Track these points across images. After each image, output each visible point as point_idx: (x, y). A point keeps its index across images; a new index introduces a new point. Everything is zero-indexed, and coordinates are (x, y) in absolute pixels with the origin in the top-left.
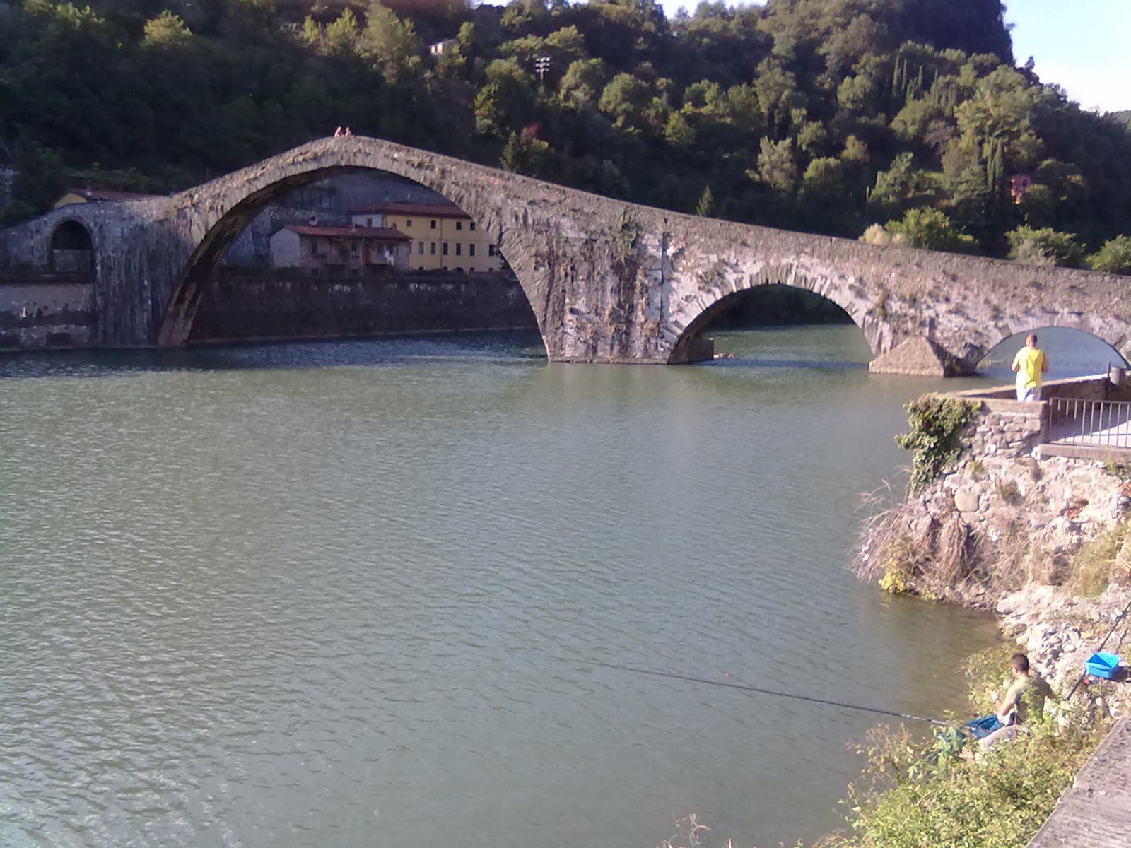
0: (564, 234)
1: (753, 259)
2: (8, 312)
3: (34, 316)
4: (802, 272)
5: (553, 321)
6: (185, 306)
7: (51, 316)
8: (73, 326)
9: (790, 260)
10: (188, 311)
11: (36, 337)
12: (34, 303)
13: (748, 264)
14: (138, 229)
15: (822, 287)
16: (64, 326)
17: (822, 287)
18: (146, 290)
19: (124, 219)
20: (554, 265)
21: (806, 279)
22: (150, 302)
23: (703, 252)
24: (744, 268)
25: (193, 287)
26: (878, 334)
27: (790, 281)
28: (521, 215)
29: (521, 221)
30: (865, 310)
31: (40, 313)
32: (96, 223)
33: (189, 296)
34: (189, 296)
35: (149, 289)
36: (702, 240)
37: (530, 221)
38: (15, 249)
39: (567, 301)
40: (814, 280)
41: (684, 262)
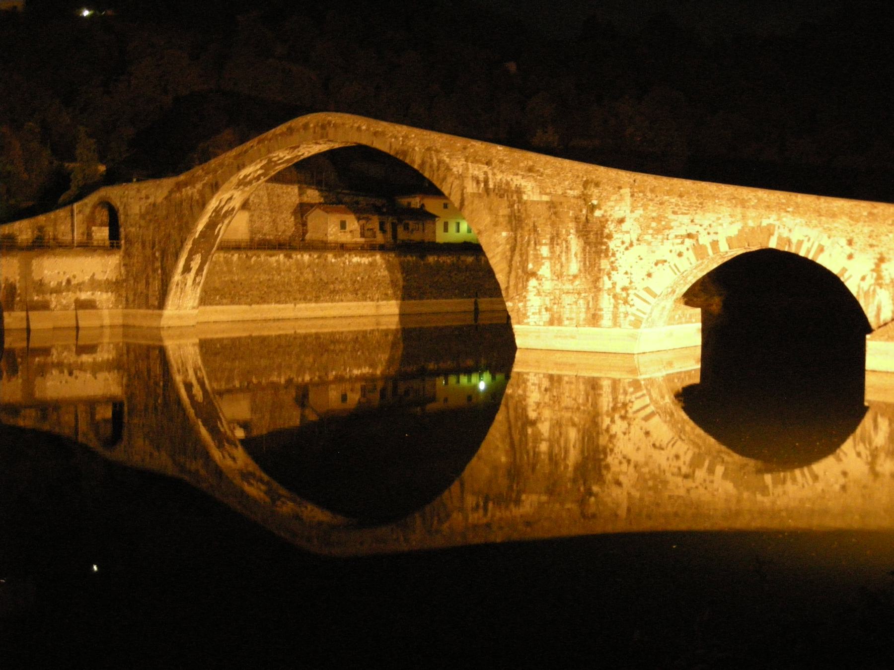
0: (525, 197)
1: (730, 220)
3: (64, 284)
4: (785, 234)
5: (516, 285)
8: (99, 293)
9: (771, 221)
10: (195, 280)
12: (64, 273)
13: (725, 225)
14: (152, 206)
15: (808, 251)
17: (808, 251)
18: (157, 260)
19: (142, 198)
20: (516, 230)
21: (789, 242)
22: (160, 271)
23: (674, 213)
24: (719, 229)
25: (198, 259)
26: (876, 303)
27: (773, 244)
28: (482, 177)
29: (482, 185)
30: (860, 277)
32: (121, 203)
33: (195, 265)
34: (195, 265)
35: (159, 259)
36: (673, 200)
37: (491, 186)
39: (530, 266)
40: (800, 243)
41: (654, 224)
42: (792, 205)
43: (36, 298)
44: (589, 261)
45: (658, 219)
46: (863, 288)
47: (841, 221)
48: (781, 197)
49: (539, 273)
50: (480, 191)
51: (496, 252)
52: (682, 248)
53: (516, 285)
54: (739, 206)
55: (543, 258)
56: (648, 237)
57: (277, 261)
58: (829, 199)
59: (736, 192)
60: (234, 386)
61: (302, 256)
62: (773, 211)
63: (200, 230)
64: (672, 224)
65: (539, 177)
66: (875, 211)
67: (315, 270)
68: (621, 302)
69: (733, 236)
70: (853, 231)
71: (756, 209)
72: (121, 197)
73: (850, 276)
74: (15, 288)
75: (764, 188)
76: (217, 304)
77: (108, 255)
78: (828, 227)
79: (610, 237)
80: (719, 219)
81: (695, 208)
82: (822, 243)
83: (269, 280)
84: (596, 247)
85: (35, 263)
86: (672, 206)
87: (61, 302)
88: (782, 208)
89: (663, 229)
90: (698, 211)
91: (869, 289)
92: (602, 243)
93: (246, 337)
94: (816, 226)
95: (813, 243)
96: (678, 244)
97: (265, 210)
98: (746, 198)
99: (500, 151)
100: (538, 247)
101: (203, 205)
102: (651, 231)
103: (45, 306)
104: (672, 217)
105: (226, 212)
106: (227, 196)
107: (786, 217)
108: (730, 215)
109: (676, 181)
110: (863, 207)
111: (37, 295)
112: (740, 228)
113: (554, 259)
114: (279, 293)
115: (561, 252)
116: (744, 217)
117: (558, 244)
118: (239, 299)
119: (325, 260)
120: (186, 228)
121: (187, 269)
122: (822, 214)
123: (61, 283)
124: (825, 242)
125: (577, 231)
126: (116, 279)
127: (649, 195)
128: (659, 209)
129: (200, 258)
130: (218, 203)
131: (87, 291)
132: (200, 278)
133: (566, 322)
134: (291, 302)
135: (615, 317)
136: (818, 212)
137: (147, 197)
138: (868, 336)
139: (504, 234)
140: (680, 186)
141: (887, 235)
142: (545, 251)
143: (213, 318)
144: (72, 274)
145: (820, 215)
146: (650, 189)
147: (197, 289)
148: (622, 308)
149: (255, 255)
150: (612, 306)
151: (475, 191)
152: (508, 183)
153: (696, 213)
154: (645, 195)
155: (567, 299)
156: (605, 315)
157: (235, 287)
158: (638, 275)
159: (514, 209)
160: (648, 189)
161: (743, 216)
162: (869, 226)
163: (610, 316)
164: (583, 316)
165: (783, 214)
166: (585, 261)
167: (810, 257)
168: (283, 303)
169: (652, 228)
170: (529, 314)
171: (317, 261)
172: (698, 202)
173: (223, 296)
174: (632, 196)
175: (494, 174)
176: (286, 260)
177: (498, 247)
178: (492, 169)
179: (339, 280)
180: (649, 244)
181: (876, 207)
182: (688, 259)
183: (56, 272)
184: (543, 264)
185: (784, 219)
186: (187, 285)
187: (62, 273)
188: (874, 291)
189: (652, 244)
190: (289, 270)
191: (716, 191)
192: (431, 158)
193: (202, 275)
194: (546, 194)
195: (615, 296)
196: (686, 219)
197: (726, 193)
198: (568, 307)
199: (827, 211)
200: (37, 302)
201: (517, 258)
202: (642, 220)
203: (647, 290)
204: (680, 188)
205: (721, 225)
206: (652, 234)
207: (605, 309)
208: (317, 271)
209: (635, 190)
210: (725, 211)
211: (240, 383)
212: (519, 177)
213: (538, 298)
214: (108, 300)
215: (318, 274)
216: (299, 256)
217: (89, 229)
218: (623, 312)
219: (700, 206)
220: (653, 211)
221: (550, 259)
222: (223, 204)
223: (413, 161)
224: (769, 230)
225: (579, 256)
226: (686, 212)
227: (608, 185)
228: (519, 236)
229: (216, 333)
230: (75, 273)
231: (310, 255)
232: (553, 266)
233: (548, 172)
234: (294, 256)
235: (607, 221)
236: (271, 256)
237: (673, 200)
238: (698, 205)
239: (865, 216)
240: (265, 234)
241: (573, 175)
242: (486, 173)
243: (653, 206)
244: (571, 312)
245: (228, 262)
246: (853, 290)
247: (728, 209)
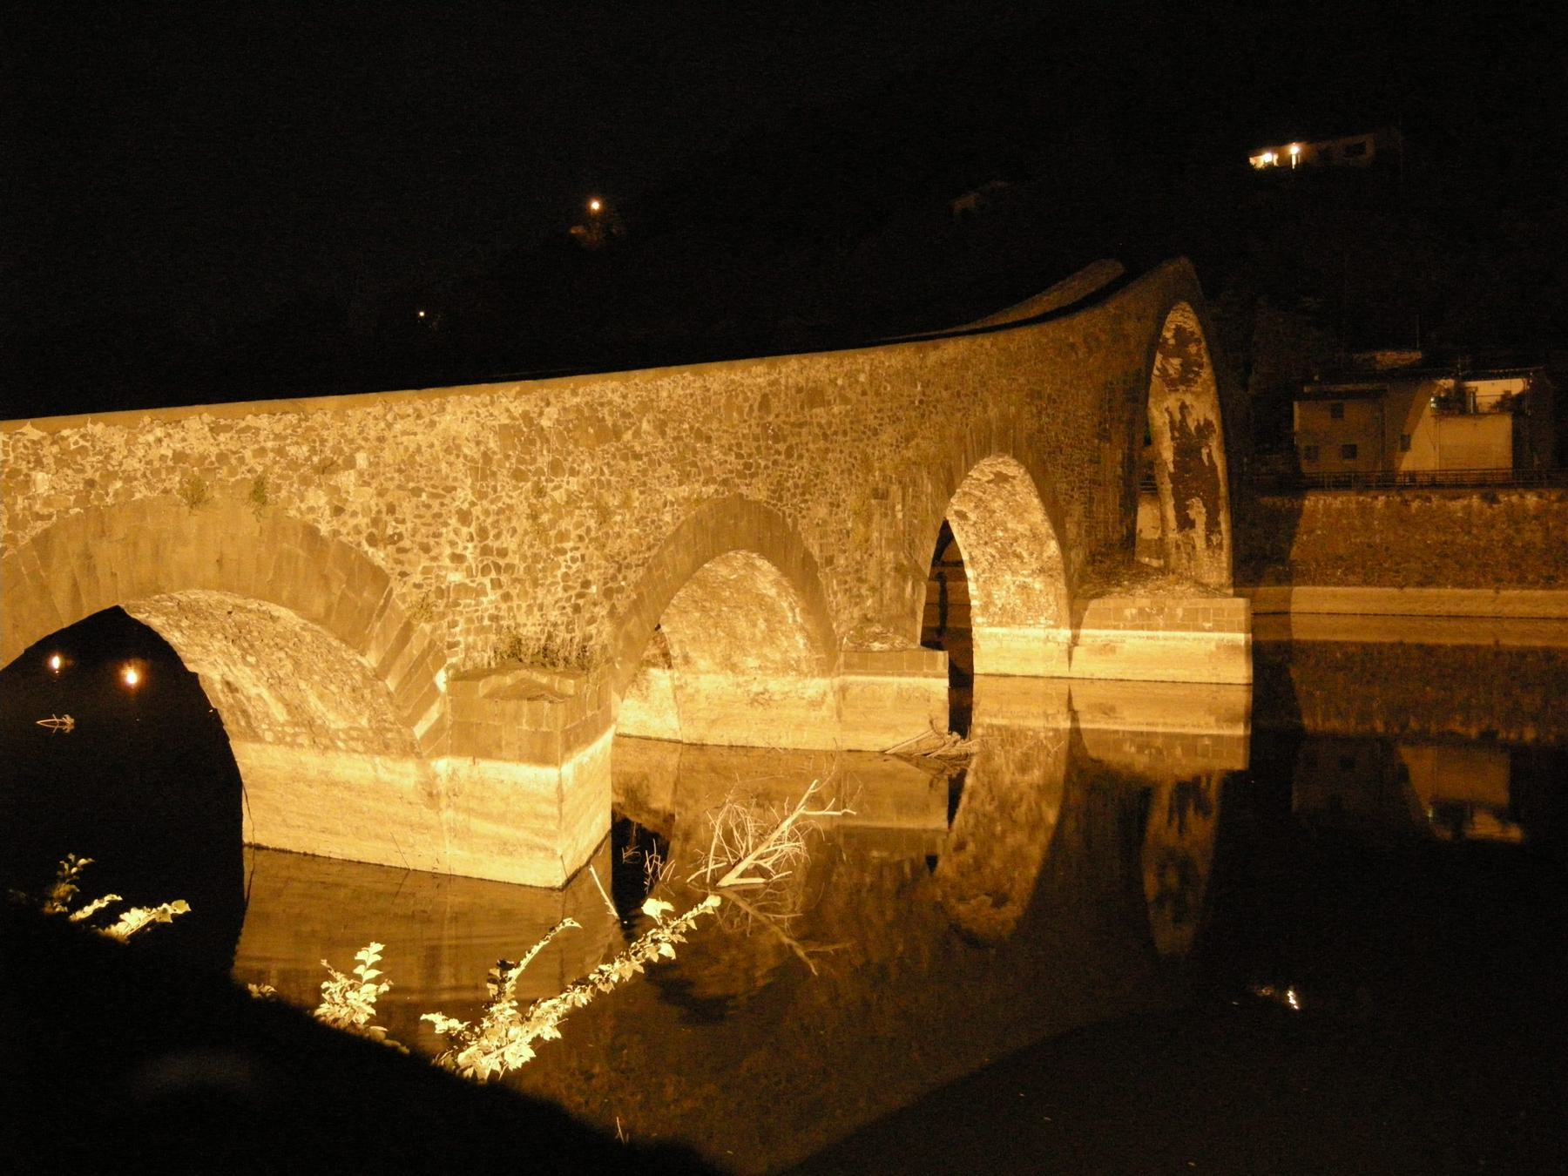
10: (1208, 539)
57: (1468, 509)
60: (1374, 729)
61: (1522, 497)
63: (1172, 459)
67: (1551, 524)
76: (1337, 584)
83: (1445, 543)
93: (1393, 645)
105: (1198, 428)
114: (1463, 567)
118: (1379, 576)
129: (1201, 504)
130: (1166, 415)
134: (1488, 586)
143: (1327, 607)
147: (1220, 554)
149: (1418, 497)
168: (1469, 588)
171: (1556, 506)
173: (1349, 570)
186: (1198, 549)
190: (1490, 525)
208: (1555, 527)
211: (1386, 724)
216: (1515, 499)
222: (1178, 417)
229: (1335, 632)
234: (1503, 498)
245: (1364, 510)
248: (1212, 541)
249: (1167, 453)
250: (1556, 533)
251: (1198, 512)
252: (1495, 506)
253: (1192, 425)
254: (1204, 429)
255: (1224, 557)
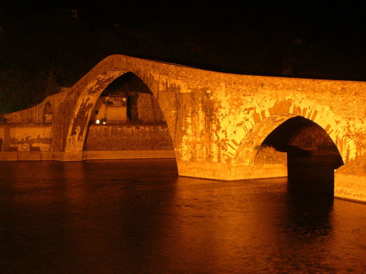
0: (181, 91)
2: (14, 138)
3: (25, 140)
6: (77, 136)
7: (32, 140)
8: (42, 144)
9: (290, 97)
10: (79, 138)
11: (25, 148)
12: (25, 135)
16: (38, 144)
21: (299, 109)
23: (244, 95)
26: (346, 148)
28: (165, 83)
31: (27, 138)
36: (243, 88)
38: (35, 115)
39: (183, 128)
40: (305, 110)
41: (236, 103)
42: (300, 86)
43: (11, 146)
44: (208, 125)
45: (237, 99)
46: (339, 138)
47: (326, 95)
48: (295, 81)
49: (187, 132)
50: (165, 90)
51: (170, 122)
52: (248, 116)
53: (178, 139)
54: (274, 89)
55: (189, 124)
56: (233, 110)
57: (132, 130)
58: (320, 81)
59: (272, 81)
62: (291, 91)
64: (244, 102)
65: (187, 80)
66: (345, 87)
68: (221, 148)
69: (271, 107)
70: (333, 101)
71: (283, 90)
72: (53, 100)
73: (332, 130)
74: (2, 140)
75: (323, 79)
77: (46, 127)
78: (320, 99)
79: (217, 111)
80: (265, 97)
81: (254, 92)
82: (317, 109)
83: (127, 139)
84: (210, 117)
85: (11, 130)
86: (243, 92)
87: (24, 148)
88: (295, 88)
89: (240, 106)
90: (255, 94)
91: (342, 139)
92: (212, 115)
94: (313, 99)
95: (312, 110)
96: (246, 114)
97: (150, 107)
98: (277, 84)
99: (173, 67)
100: (186, 118)
101: (75, 102)
102: (234, 107)
103: (15, 149)
104: (243, 97)
106: (86, 98)
107: (297, 94)
108: (270, 95)
109: (245, 77)
110: (338, 84)
111: (12, 145)
112: (275, 102)
113: (193, 125)
115: (195, 120)
116: (277, 96)
117: (194, 116)
119: (157, 130)
120: (71, 114)
121: (74, 133)
122: (316, 91)
123: (23, 139)
124: (319, 108)
125: (203, 109)
126: (50, 138)
127: (233, 85)
128: (238, 93)
131: (36, 143)
132: (82, 137)
133: (198, 160)
135: (219, 157)
136: (314, 89)
137: (60, 100)
138: (335, 170)
139: (173, 112)
140: (246, 79)
141: (352, 102)
142: (189, 120)
144: (29, 135)
145: (315, 92)
146: (233, 82)
147: (81, 143)
148: (222, 152)
150: (217, 150)
151: (163, 90)
152: (175, 84)
153: (254, 95)
154: (231, 86)
155: (198, 146)
156: (214, 156)
157: (109, 142)
158: (229, 133)
159: (177, 98)
160: (232, 82)
161: (276, 95)
162: (342, 97)
163: (217, 156)
164: (205, 156)
165: (296, 92)
166: (206, 125)
167: (310, 119)
169: (235, 105)
170: (183, 155)
172: (255, 88)
174: (226, 87)
175: (170, 80)
176: (137, 130)
177: (171, 118)
178: (169, 77)
179: (165, 139)
180: (234, 114)
181: (345, 84)
182: (251, 122)
183: (21, 134)
184: (188, 127)
185: (297, 95)
186: (75, 141)
187: (24, 135)
188: (346, 139)
189: (236, 114)
191: (263, 81)
192: (147, 74)
193: (83, 136)
194: (190, 89)
195: (219, 145)
196: (249, 99)
197: (268, 81)
198: (199, 151)
199: (318, 88)
200: (12, 148)
201: (178, 125)
202: (230, 100)
203: (233, 141)
204: (247, 80)
205: (266, 101)
206: (235, 108)
207: (214, 153)
209: (227, 84)
210: (268, 92)
212: (179, 80)
213: (186, 146)
214: (45, 148)
215: (153, 136)
217: (44, 115)
218: (222, 154)
219: (256, 90)
220: (235, 95)
221: (191, 124)
222: (85, 102)
223: (141, 76)
224: (289, 103)
225: (203, 122)
226: (249, 94)
227: (215, 82)
228: (179, 112)
230: (30, 135)
231: (149, 127)
232: (192, 128)
233: (191, 77)
234: (141, 128)
235: (215, 102)
236: (129, 127)
237: (243, 88)
238: (255, 90)
239: (339, 90)
240: (149, 119)
241: (201, 77)
242: (167, 79)
243: (235, 92)
244: (200, 154)
246: (334, 140)
247: (269, 91)
248: (80, 138)
249: (76, 112)
250: (153, 136)
251: (78, 130)
252: (139, 130)
253: (87, 104)
254: (90, 105)
255: (82, 143)
